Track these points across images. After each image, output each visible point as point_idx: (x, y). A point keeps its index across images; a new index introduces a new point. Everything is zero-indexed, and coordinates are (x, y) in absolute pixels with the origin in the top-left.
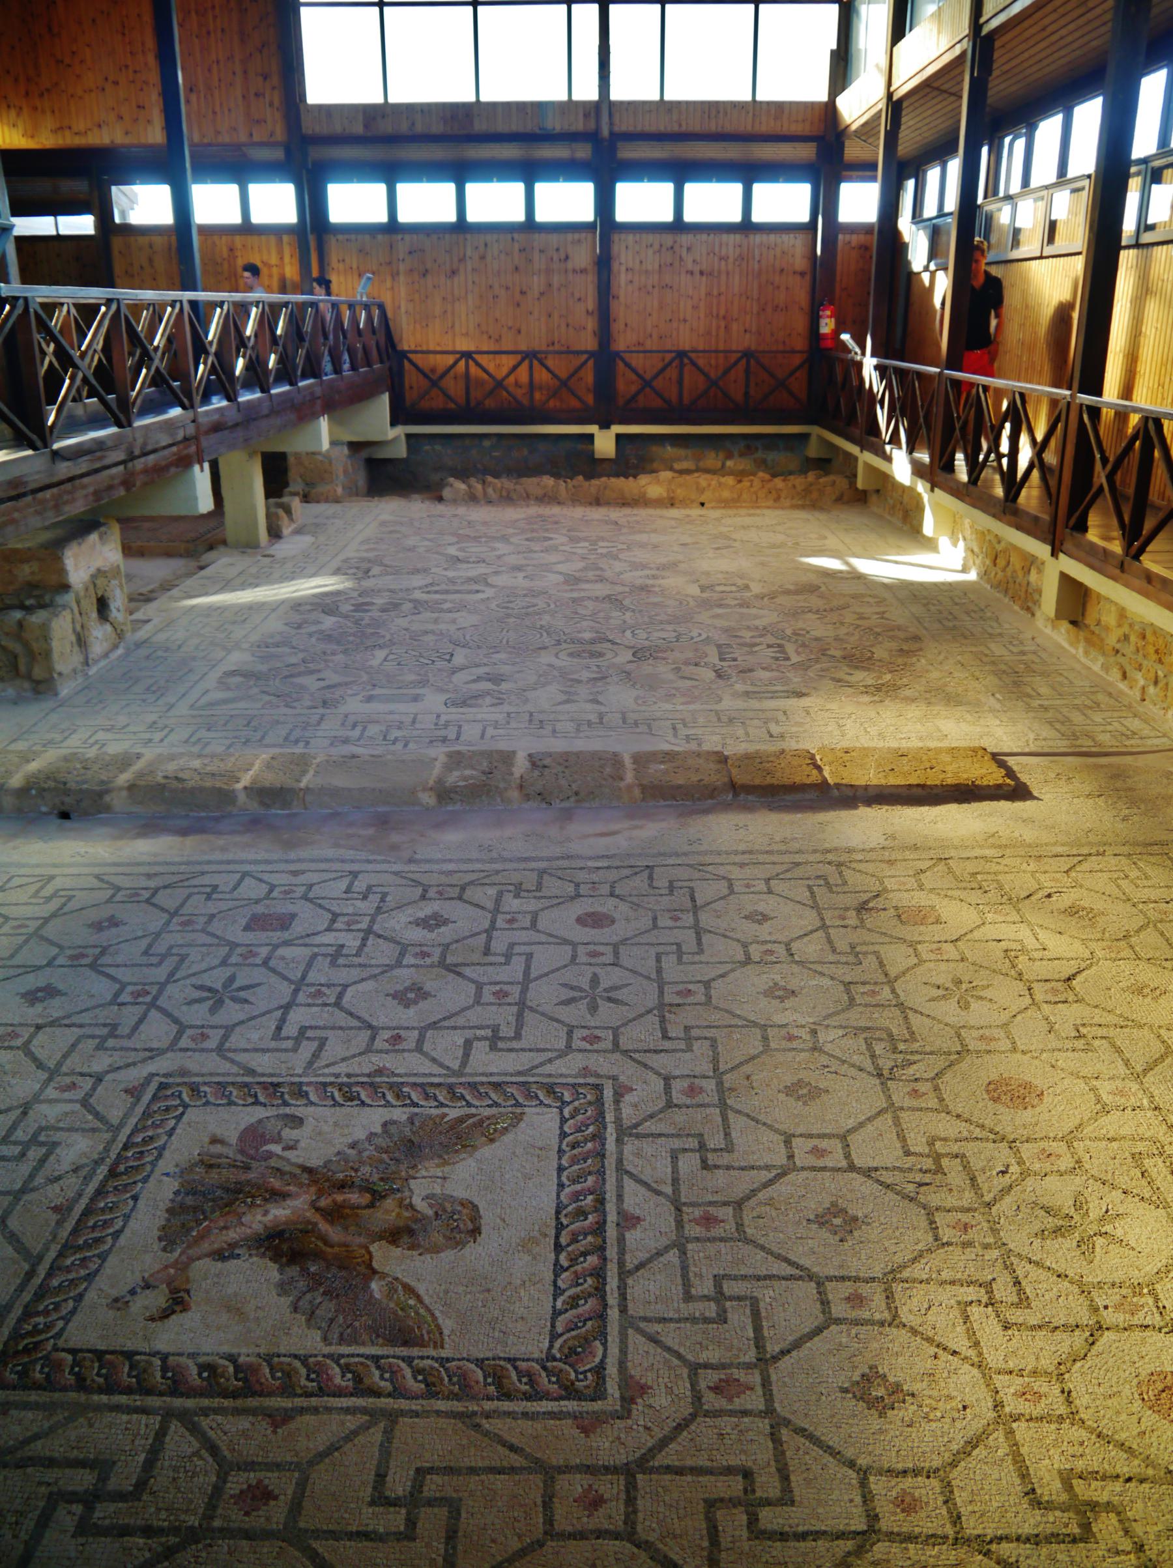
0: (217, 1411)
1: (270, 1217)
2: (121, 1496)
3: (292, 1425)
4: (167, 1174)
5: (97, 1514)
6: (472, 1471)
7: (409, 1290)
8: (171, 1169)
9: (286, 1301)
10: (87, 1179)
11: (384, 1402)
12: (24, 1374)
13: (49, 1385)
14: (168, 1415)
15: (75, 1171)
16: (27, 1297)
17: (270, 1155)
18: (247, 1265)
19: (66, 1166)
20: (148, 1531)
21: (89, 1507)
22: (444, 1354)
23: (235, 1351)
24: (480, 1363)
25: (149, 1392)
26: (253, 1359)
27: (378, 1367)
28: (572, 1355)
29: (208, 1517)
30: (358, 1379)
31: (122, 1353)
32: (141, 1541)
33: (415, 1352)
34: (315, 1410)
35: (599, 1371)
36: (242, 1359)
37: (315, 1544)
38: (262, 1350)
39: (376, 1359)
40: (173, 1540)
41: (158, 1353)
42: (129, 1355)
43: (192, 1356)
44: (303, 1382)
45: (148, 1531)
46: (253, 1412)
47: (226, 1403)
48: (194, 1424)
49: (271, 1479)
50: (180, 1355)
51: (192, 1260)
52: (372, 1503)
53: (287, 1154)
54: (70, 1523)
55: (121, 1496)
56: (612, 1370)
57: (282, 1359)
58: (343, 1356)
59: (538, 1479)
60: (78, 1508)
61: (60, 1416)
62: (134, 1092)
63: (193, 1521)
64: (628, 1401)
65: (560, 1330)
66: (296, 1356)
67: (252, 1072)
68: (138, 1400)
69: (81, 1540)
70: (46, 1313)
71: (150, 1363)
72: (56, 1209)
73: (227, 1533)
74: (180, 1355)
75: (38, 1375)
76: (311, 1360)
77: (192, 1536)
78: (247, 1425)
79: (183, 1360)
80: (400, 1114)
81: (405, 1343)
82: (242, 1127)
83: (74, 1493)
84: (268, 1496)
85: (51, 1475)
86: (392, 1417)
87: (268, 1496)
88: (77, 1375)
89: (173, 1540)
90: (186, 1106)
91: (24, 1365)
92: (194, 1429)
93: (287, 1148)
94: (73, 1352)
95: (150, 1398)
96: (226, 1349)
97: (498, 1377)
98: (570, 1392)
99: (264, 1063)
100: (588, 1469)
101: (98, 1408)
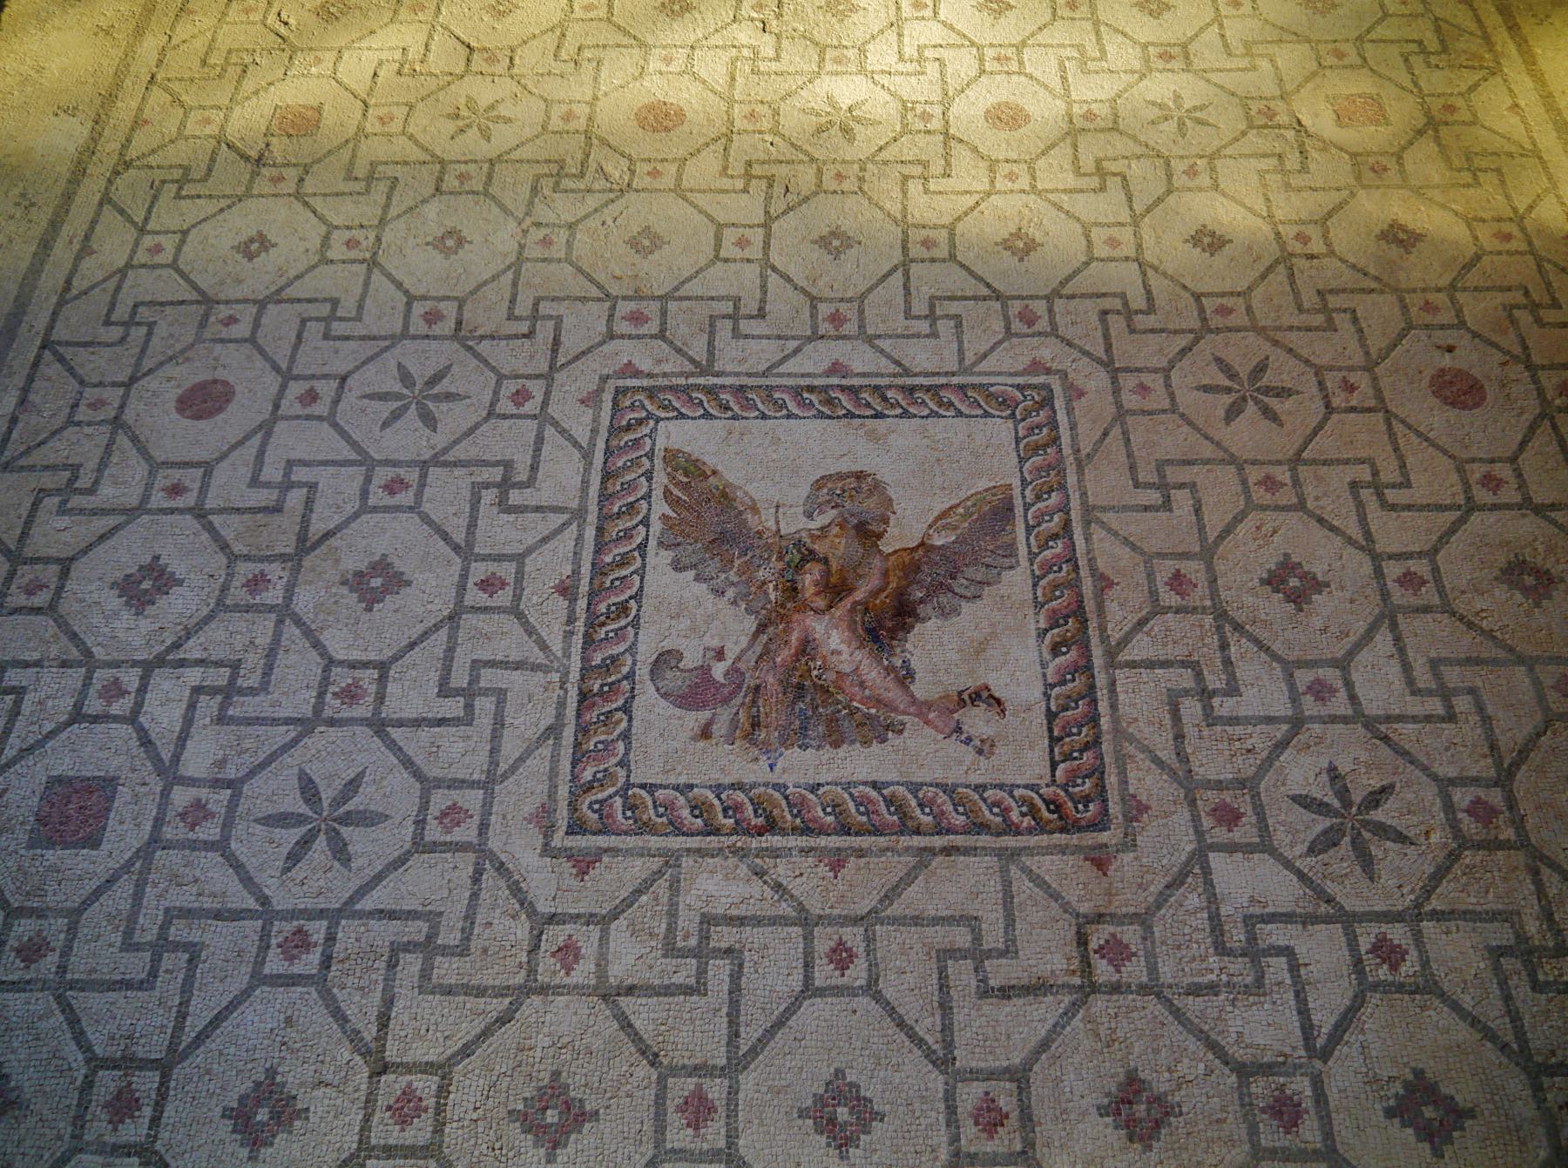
0: (1102, 629)
1: (843, 647)
2: (1199, 675)
3: (1109, 572)
4: (771, 767)
5: (1218, 686)
6: (1130, 455)
7: (943, 515)
8: (764, 763)
9: (966, 607)
10: (775, 853)
11: (1075, 515)
12: (1087, 800)
13: (1098, 772)
14: (1112, 663)
15: (760, 873)
16: (984, 840)
17: (734, 671)
18: (917, 652)
19: (757, 887)
20: (1224, 646)
21: (1214, 693)
22: (1016, 482)
23: (1034, 633)
24: (1022, 461)
25: (1092, 687)
26: (1042, 617)
27: (1039, 525)
28: (1004, 402)
29: (1204, 610)
30: (1055, 537)
31: (1050, 723)
32: (1233, 649)
33: (1018, 502)
34: (1091, 561)
35: (1019, 387)
36: (1043, 625)
37: (1211, 540)
38: (1031, 611)
39: (1029, 529)
40: (1228, 628)
41: (1045, 694)
42: (1051, 716)
43: (1044, 665)
44: (1063, 573)
45: (1224, 646)
46: (1100, 607)
47: (1093, 625)
48: (1119, 644)
49: (1162, 577)
50: (1044, 675)
51: (914, 701)
52: (1170, 510)
53: (730, 655)
54: (1230, 702)
55: (1199, 675)
56: (1020, 380)
57: (1039, 593)
58: (1030, 552)
59: (1130, 420)
60: (1216, 701)
61: (1130, 749)
62: (584, 864)
63: (1208, 620)
64: (1048, 371)
65: (980, 412)
66: (1035, 585)
67: (554, 731)
68: (1102, 694)
69: (1242, 689)
70: (1006, 811)
71: (1057, 698)
72: (837, 866)
73: (1214, 594)
74: (1044, 675)
75: (1088, 785)
76: (1037, 573)
77: (1221, 615)
78: (1115, 604)
79: (1050, 670)
80: (659, 559)
81: (1011, 509)
82: (678, 712)
83: (1204, 708)
84: (1177, 575)
85: (1190, 731)
86: (1087, 509)
87: (1177, 575)
88: (1081, 751)
89: (1228, 628)
90: (629, 785)
91: (1075, 804)
92: (1124, 642)
93: (720, 654)
94: (1054, 766)
95: (1098, 684)
96: (1032, 641)
97: (1036, 449)
98: (1047, 402)
99: (526, 721)
100: (1116, 391)
101: (1116, 720)
